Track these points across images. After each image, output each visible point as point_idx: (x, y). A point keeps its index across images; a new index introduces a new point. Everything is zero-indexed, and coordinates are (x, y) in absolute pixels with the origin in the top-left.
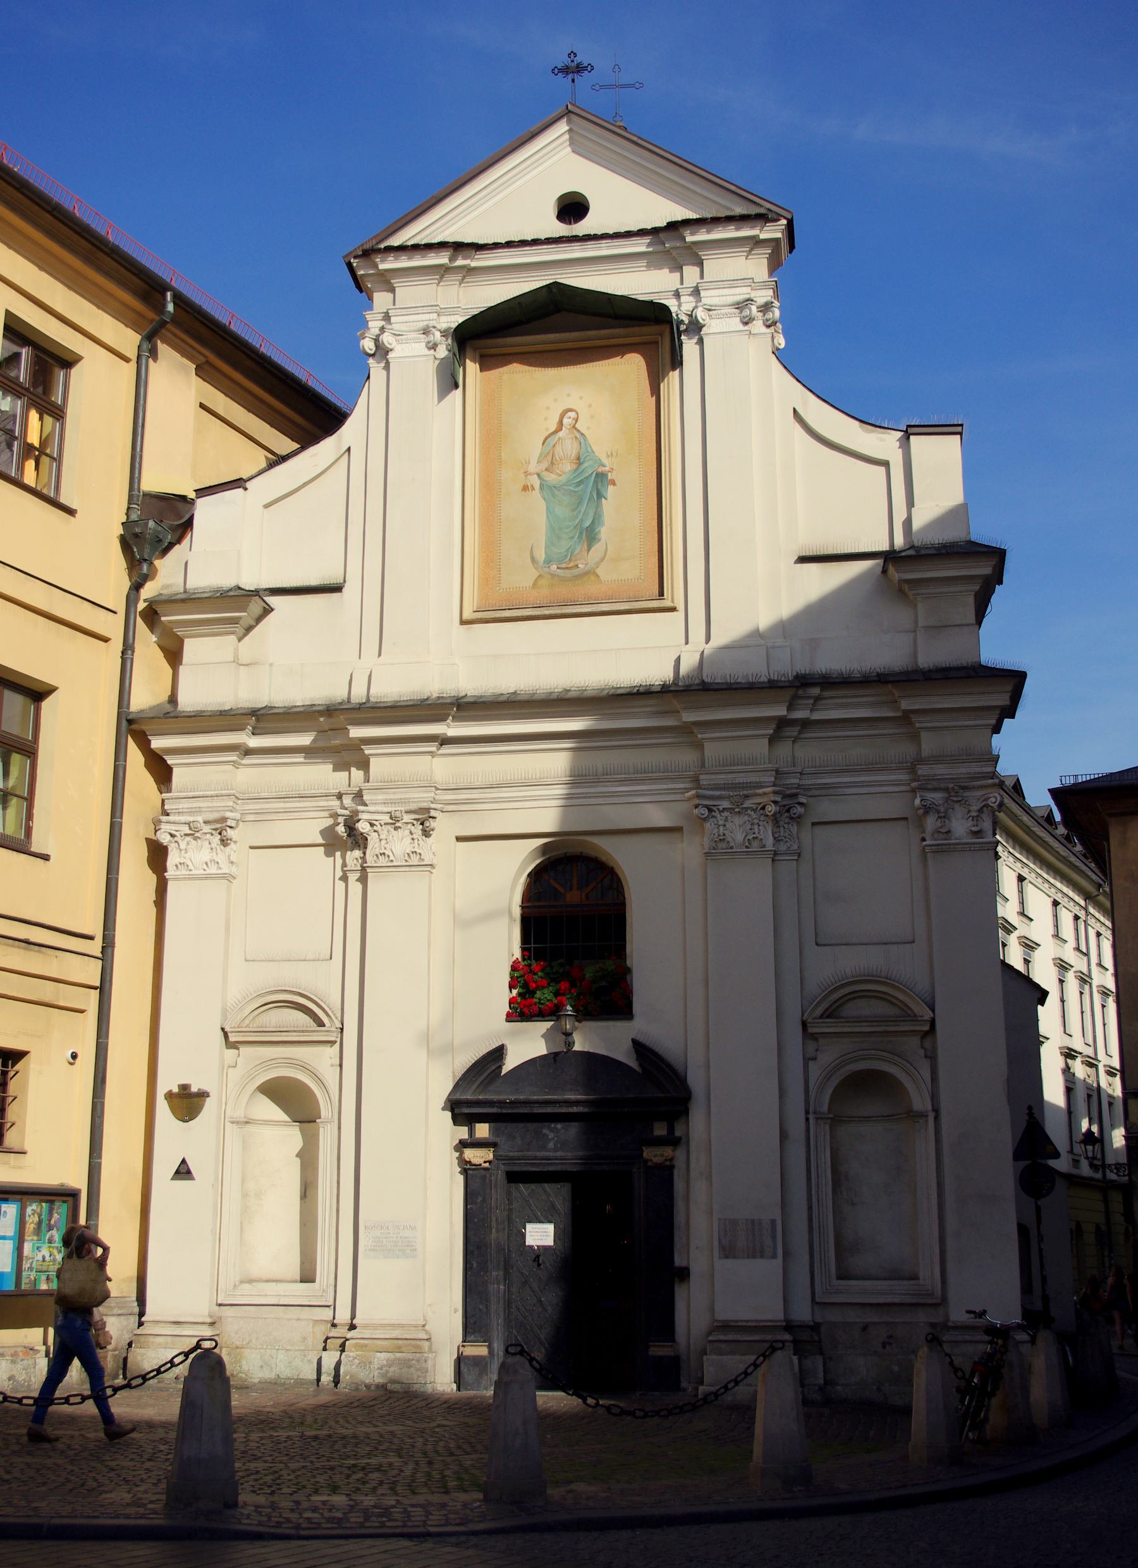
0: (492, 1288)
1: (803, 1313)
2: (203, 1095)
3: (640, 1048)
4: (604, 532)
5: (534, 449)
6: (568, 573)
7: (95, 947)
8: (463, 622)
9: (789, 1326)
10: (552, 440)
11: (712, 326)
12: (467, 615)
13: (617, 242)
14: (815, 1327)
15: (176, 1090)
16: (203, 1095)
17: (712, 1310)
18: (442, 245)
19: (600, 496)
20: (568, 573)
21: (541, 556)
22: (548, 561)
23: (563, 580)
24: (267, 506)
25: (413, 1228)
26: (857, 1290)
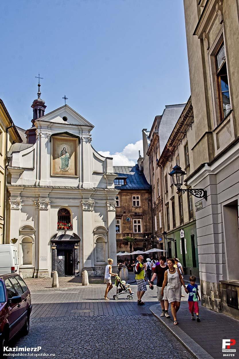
0: (56, 264)
1: (93, 266)
2: (17, 239)
3: (74, 234)
4: (69, 165)
5: (60, 153)
6: (64, 171)
7: (3, 219)
8: (51, 176)
9: (92, 268)
10: (62, 152)
11: (84, 140)
12: (52, 175)
13: (72, 126)
14: (94, 268)
15: (13, 239)
16: (17, 239)
17: (83, 266)
18: (50, 122)
19: (69, 160)
20: (64, 171)
21: (61, 168)
22: (62, 169)
23: (64, 171)
24: (23, 156)
25: (46, 257)
26: (99, 263)
